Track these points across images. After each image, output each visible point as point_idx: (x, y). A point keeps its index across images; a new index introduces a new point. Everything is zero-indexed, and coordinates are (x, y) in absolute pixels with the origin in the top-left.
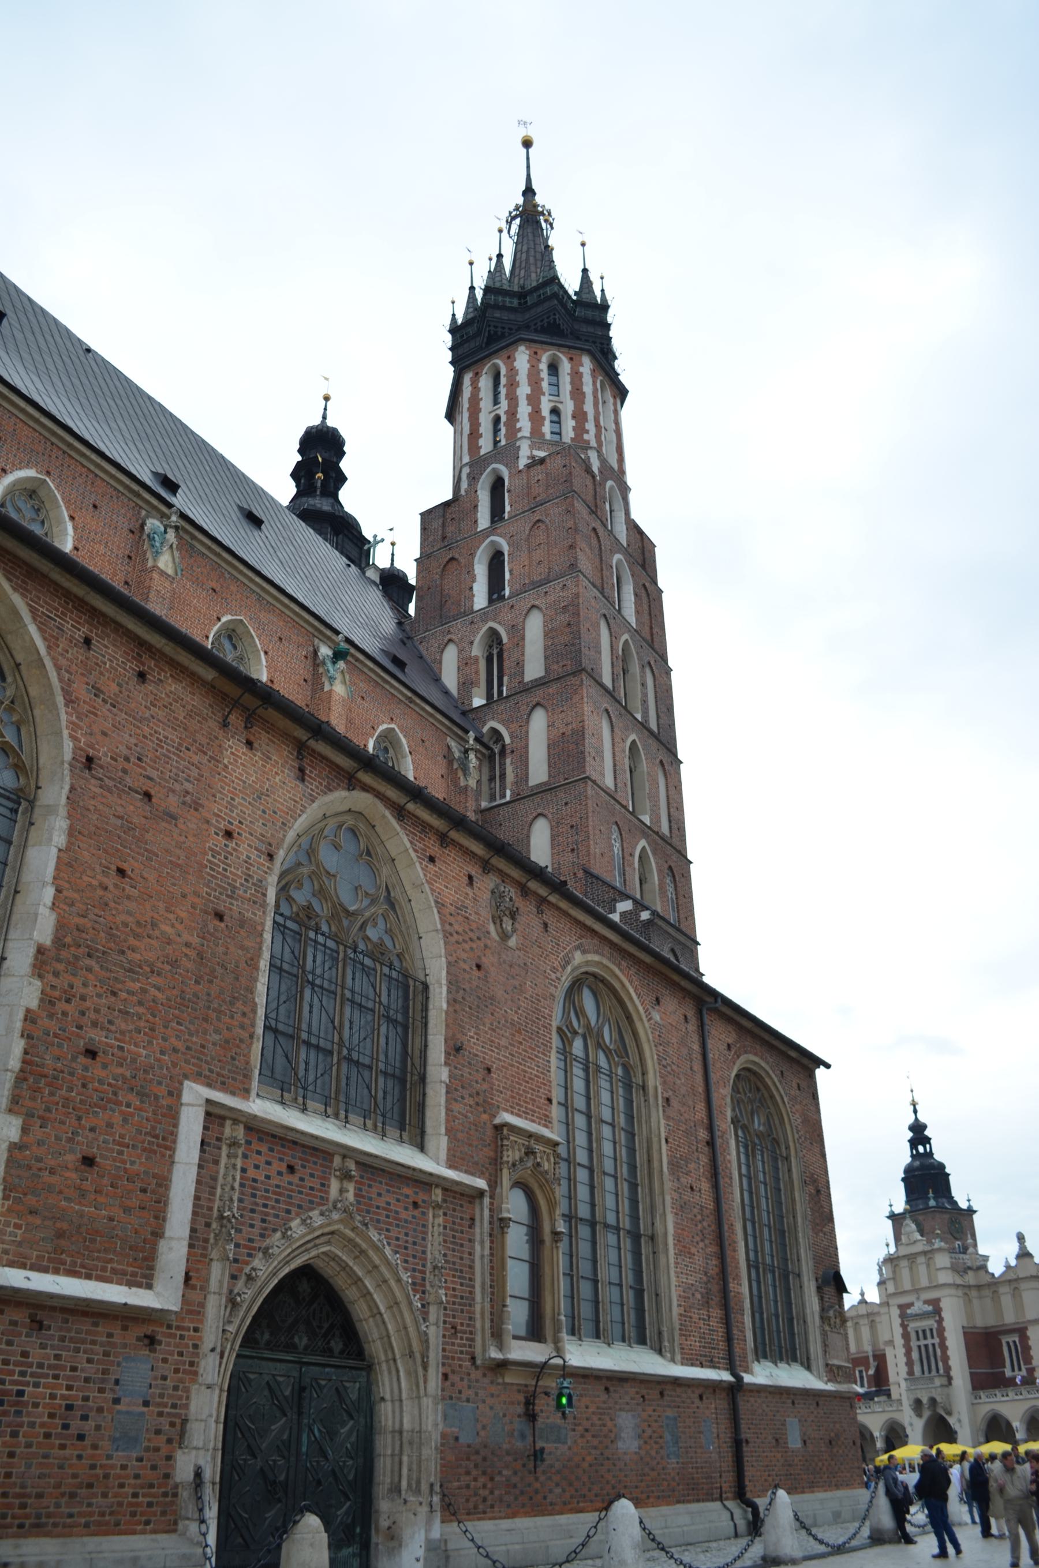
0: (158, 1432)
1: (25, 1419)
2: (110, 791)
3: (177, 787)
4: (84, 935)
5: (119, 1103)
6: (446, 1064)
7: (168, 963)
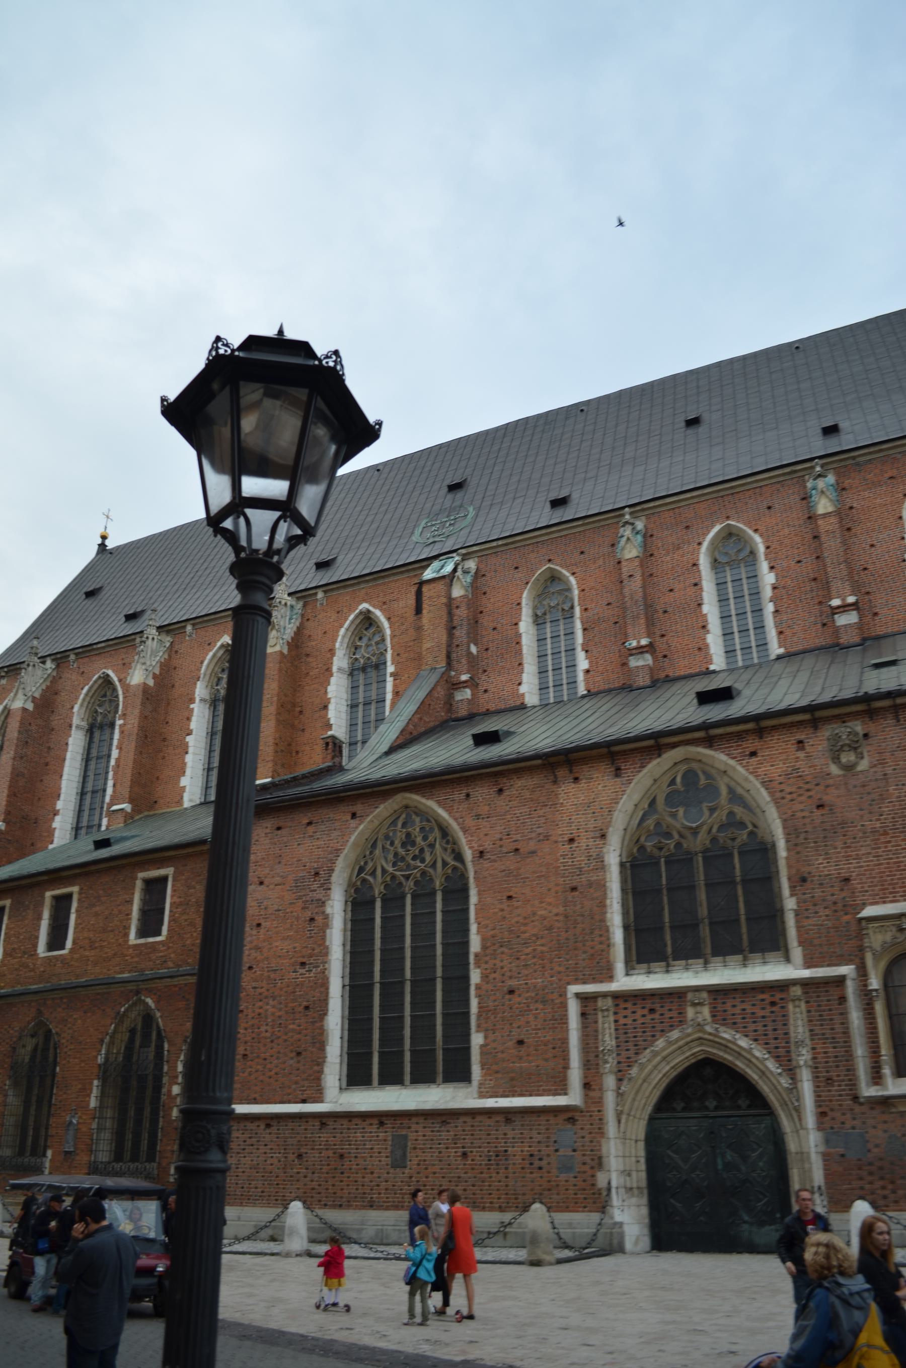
0: (584, 1164)
2: (495, 861)
3: (533, 835)
5: (531, 1010)
6: (792, 895)
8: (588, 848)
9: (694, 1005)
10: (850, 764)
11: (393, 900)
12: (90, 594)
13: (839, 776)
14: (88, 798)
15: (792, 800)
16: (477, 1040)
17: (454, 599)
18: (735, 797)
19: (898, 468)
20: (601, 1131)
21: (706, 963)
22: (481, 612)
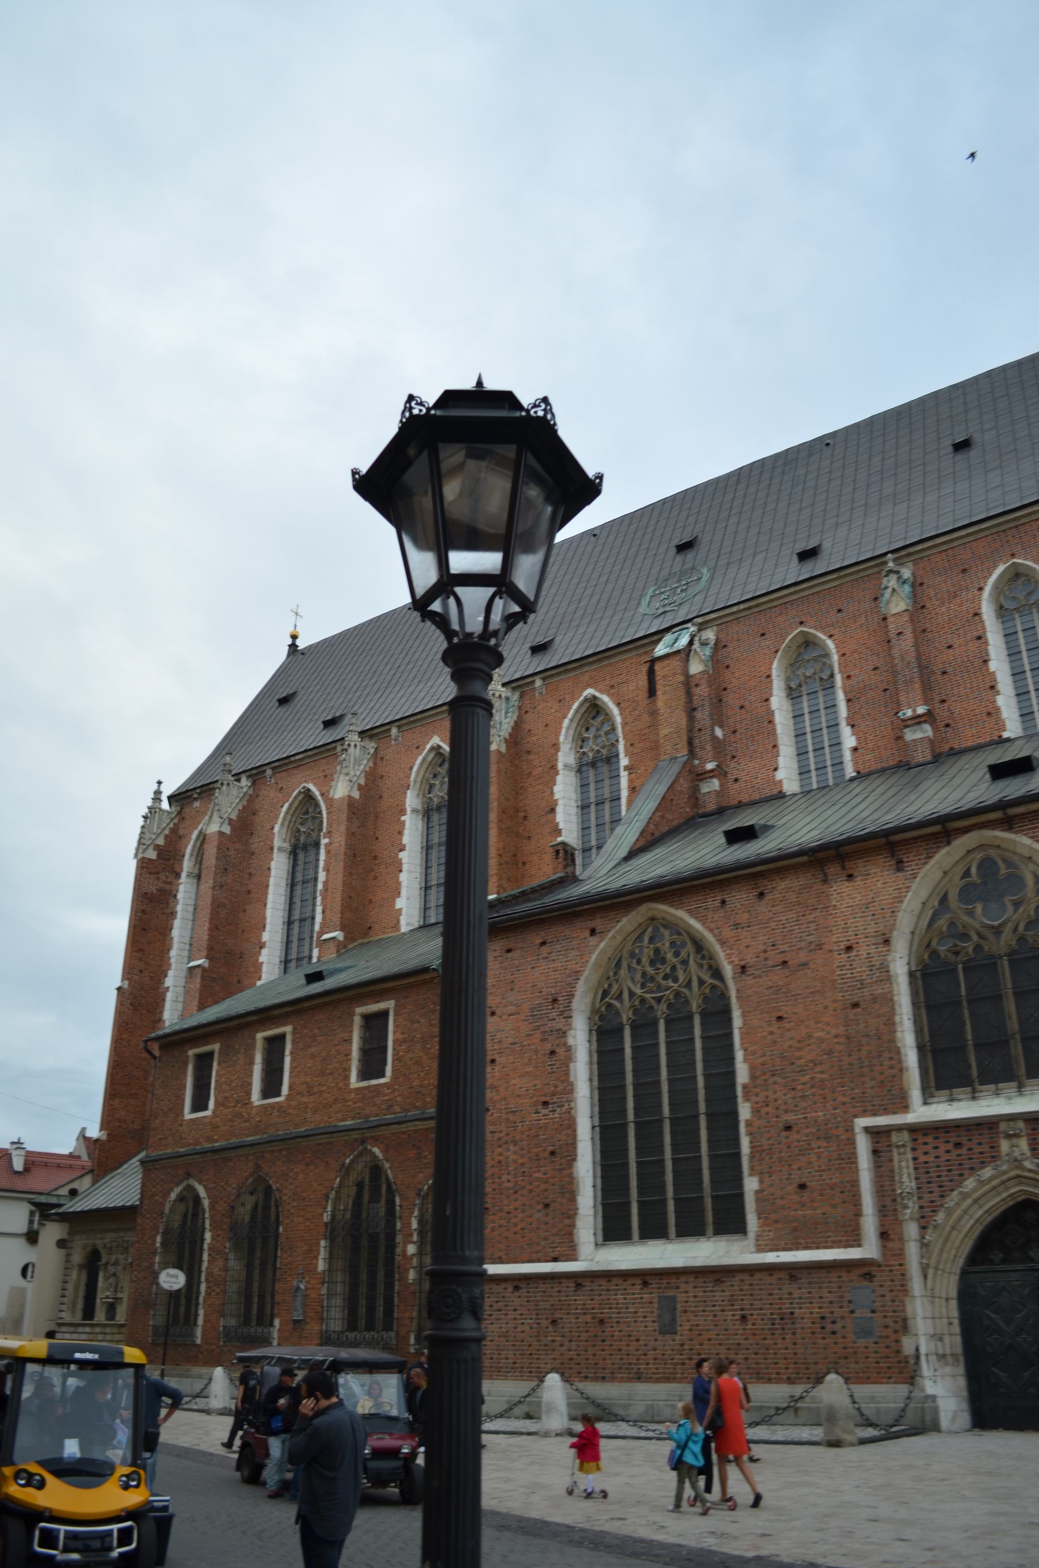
0: (886, 1327)
2: (760, 977)
3: (803, 944)
5: (813, 1149)
7: (826, 1054)
8: (869, 956)
9: (1009, 1137)
11: (644, 1027)
12: (283, 701)
14: (296, 926)
16: (751, 1185)
17: (692, 676)
20: (903, 1289)
22: (725, 689)
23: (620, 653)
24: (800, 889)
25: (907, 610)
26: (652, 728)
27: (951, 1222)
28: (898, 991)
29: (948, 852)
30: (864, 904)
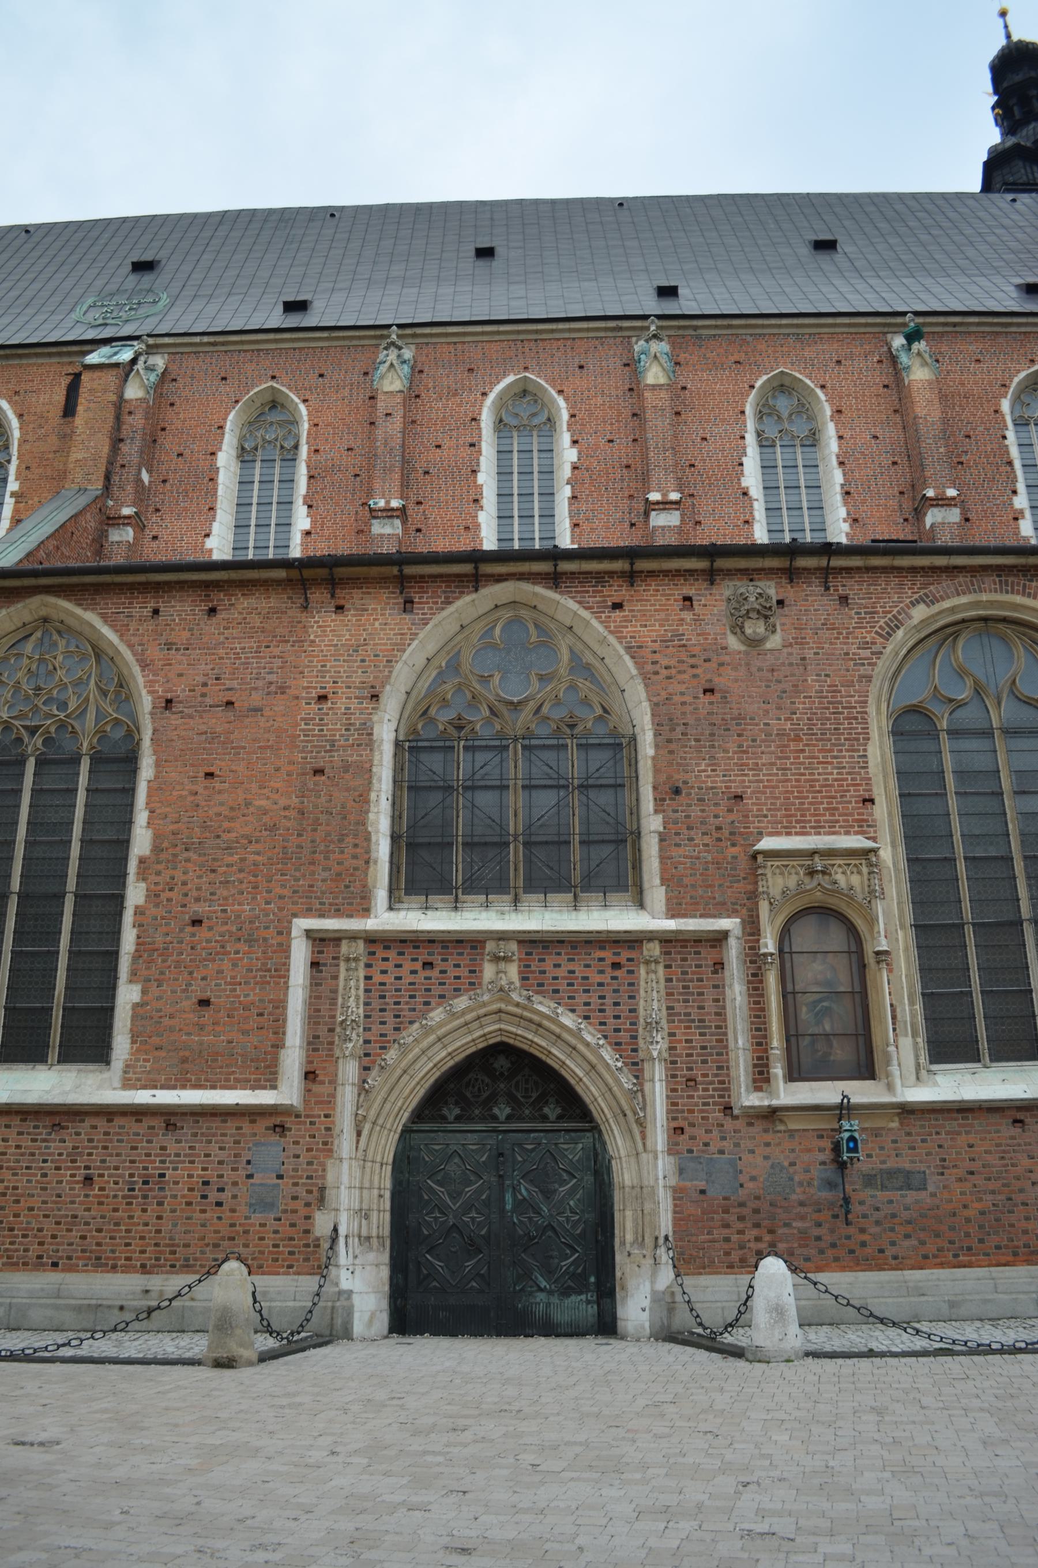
0: (295, 1198)
1: (168, 1193)
2: (191, 717)
3: (260, 683)
4: (179, 836)
6: (656, 812)
7: (266, 830)
9: (496, 959)
10: (757, 638)
13: (740, 652)
15: (669, 678)
17: (126, 401)
18: (581, 667)
19: (746, 353)
20: (328, 1148)
21: (516, 901)
22: (163, 429)
23: (37, 355)
24: (268, 613)
25: (402, 391)
26: (58, 454)
27: (403, 1065)
28: (381, 760)
29: (473, 601)
30: (352, 646)
